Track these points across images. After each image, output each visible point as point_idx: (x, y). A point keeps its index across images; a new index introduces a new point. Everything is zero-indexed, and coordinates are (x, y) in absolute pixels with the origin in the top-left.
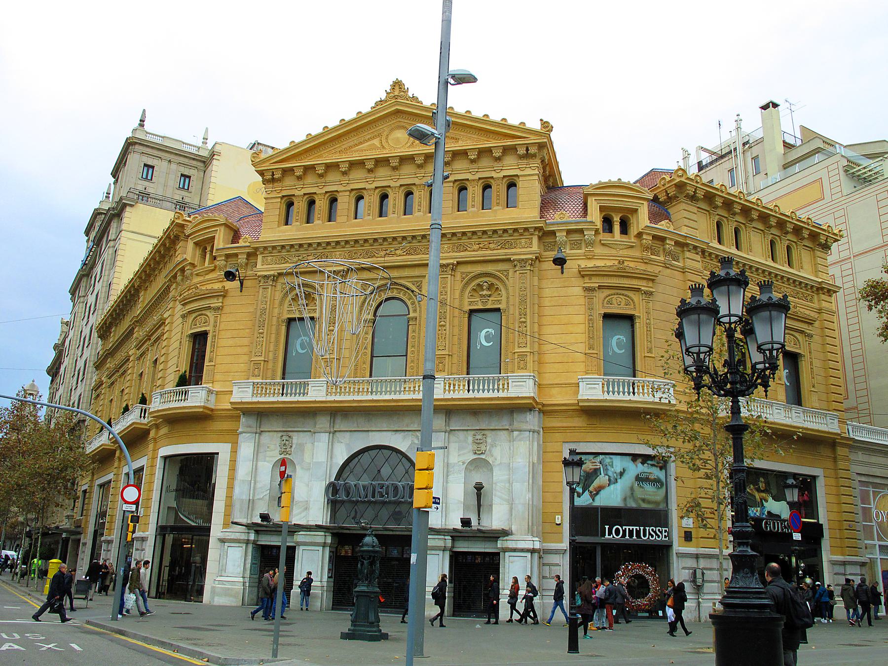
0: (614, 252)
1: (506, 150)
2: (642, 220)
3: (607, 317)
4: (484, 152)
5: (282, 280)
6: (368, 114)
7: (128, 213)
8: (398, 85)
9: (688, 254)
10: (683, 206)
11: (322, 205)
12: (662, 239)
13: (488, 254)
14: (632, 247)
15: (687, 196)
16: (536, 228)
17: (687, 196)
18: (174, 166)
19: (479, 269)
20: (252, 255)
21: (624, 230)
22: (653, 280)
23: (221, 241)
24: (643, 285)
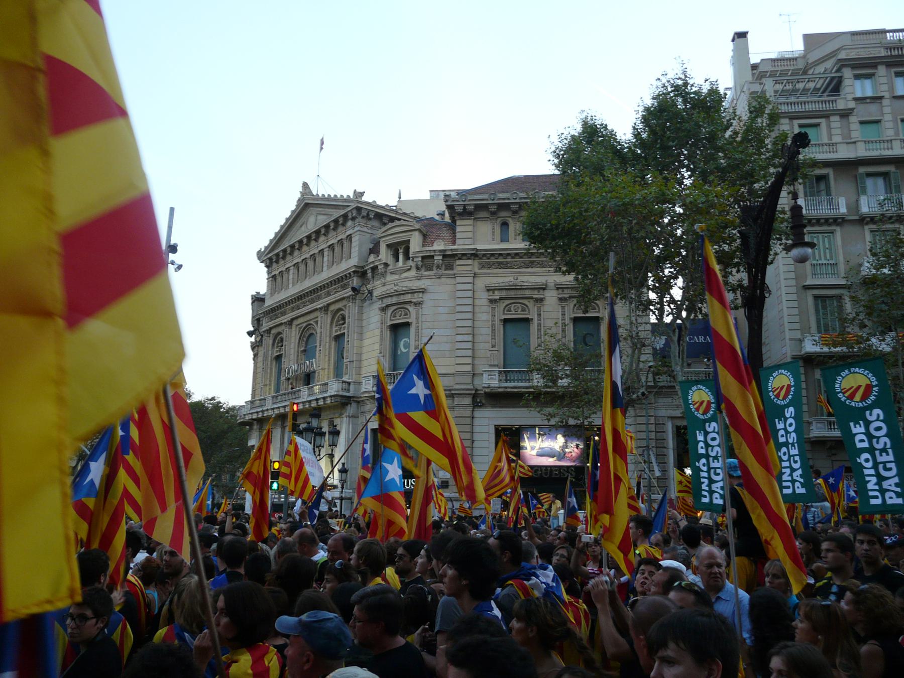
0: (397, 277)
5: (273, 331)
6: (295, 210)
8: (305, 185)
9: (458, 262)
12: (432, 257)
13: (338, 296)
14: (409, 269)
15: (460, 214)
16: (354, 272)
17: (460, 214)
21: (407, 257)
22: (423, 292)
24: (416, 298)
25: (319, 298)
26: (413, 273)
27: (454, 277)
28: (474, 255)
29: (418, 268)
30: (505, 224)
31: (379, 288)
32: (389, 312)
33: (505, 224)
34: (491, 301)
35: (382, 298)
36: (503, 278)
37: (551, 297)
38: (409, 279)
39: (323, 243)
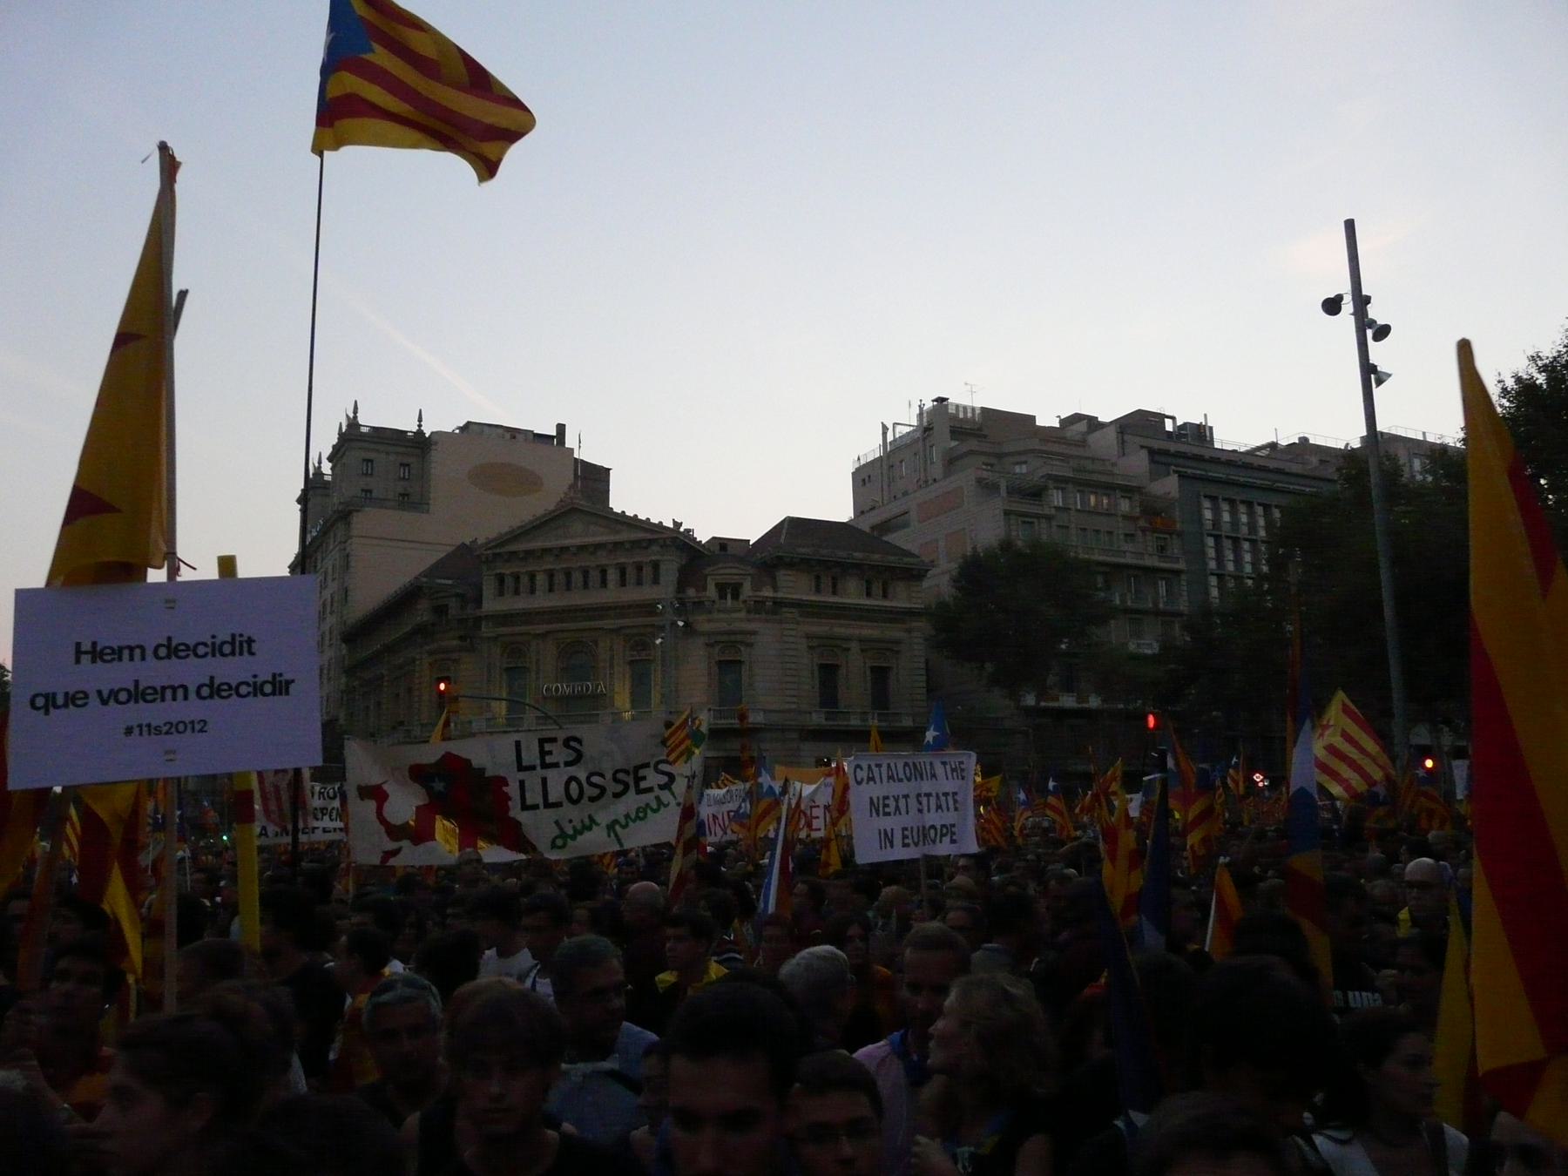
1: (651, 542)
2: (747, 591)
3: (720, 663)
4: (636, 544)
7: (356, 519)
10: (783, 572)
11: (525, 580)
18: (392, 458)
19: (635, 631)
20: (478, 620)
23: (453, 604)
25: (601, 618)
26: (743, 614)
27: (781, 622)
28: (797, 604)
29: (749, 612)
30: (818, 578)
31: (703, 623)
32: (717, 649)
33: (818, 578)
34: (811, 648)
35: (709, 634)
36: (820, 628)
37: (854, 646)
38: (741, 620)
39: (603, 559)
